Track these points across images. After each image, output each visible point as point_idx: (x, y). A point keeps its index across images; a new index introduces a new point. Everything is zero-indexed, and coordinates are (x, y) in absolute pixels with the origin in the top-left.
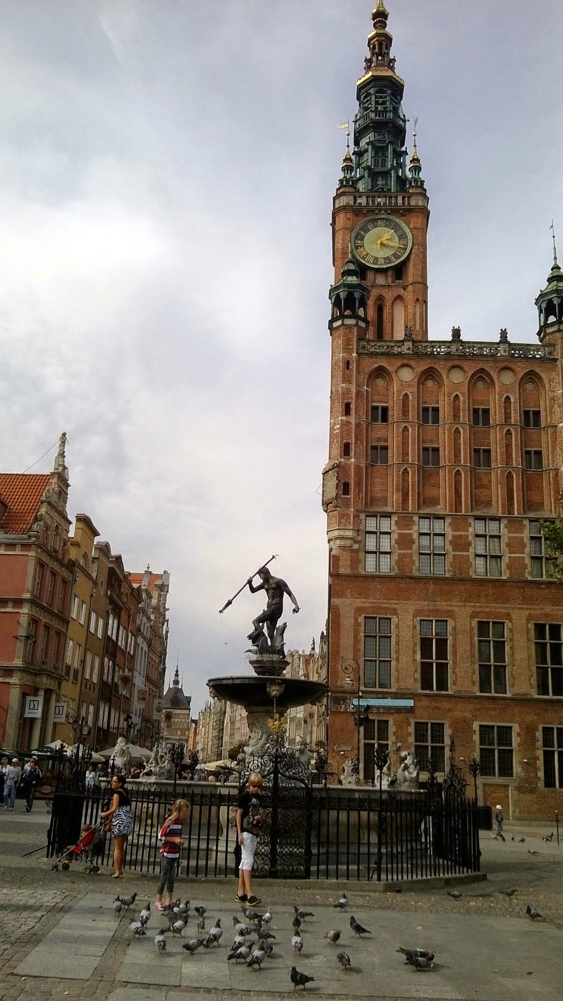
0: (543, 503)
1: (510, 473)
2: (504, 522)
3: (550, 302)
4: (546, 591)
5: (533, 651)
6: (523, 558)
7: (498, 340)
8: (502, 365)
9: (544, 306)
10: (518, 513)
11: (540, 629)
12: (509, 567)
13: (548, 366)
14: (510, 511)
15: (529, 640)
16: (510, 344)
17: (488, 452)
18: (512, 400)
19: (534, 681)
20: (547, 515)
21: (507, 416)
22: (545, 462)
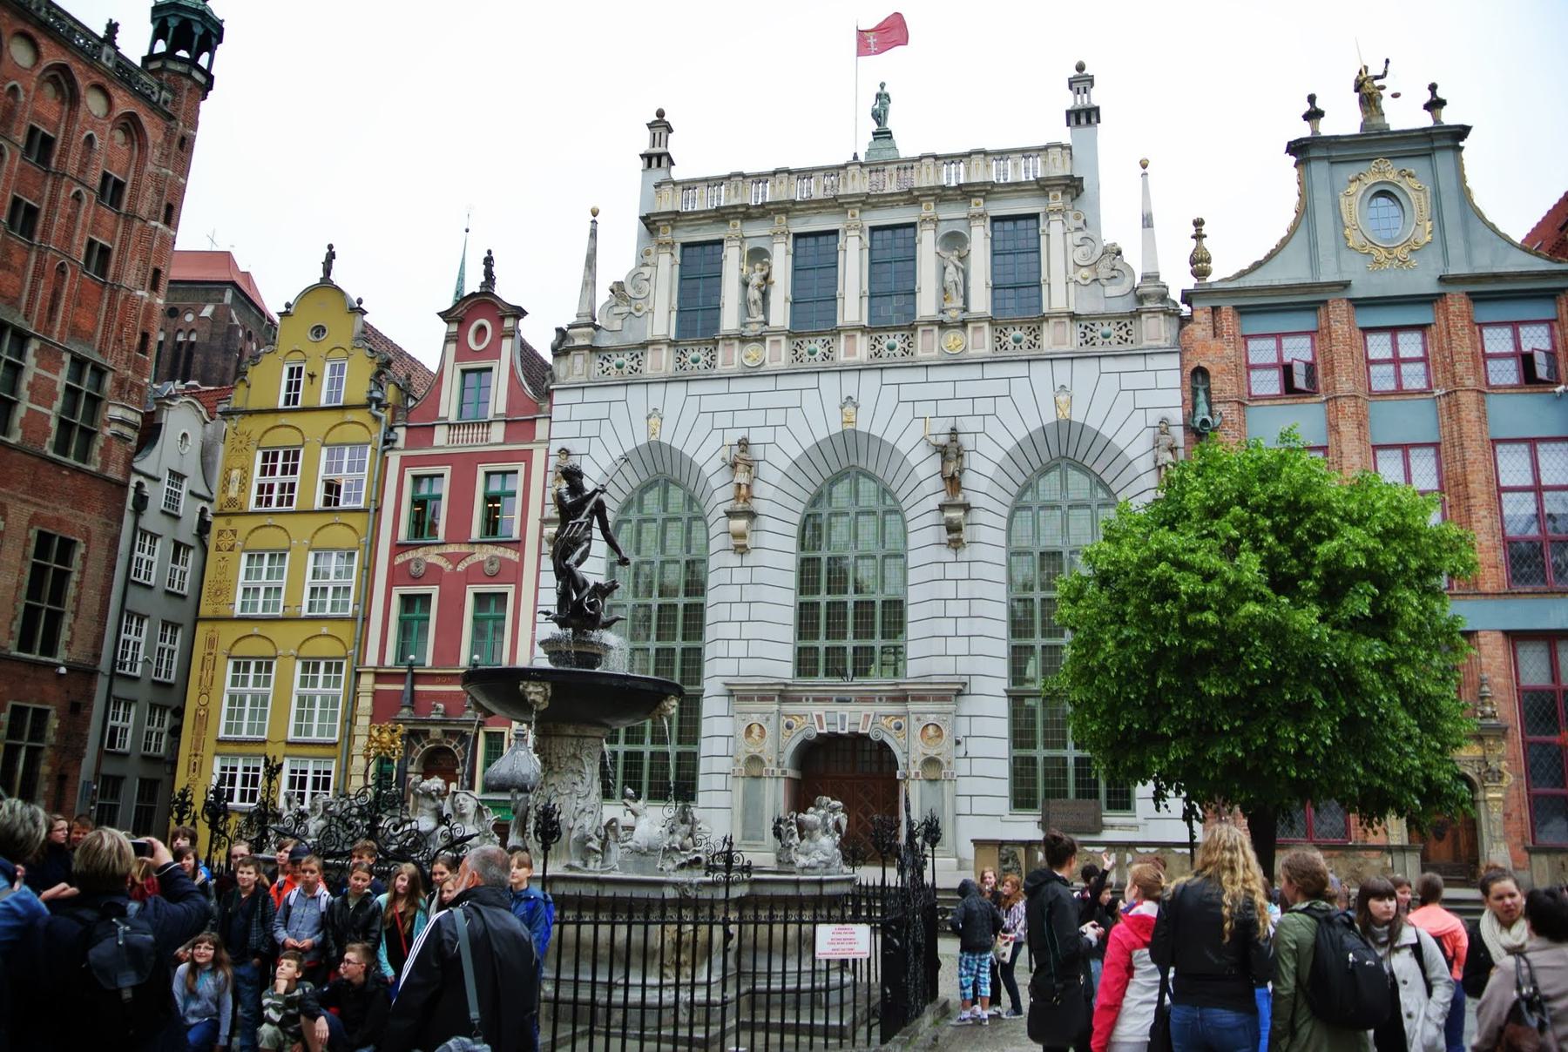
0: (92, 336)
1: (62, 265)
2: (34, 346)
3: (185, 26)
4: (68, 481)
5: (27, 578)
6: (48, 417)
7: (101, 34)
8: (96, 79)
9: (173, 23)
10: (60, 340)
11: (44, 540)
12: (25, 424)
13: (157, 120)
14: (50, 333)
15: (25, 557)
16: (118, 54)
17: (32, 212)
18: (97, 146)
19: (16, 627)
20: (97, 358)
21: (83, 169)
22: (111, 270)
